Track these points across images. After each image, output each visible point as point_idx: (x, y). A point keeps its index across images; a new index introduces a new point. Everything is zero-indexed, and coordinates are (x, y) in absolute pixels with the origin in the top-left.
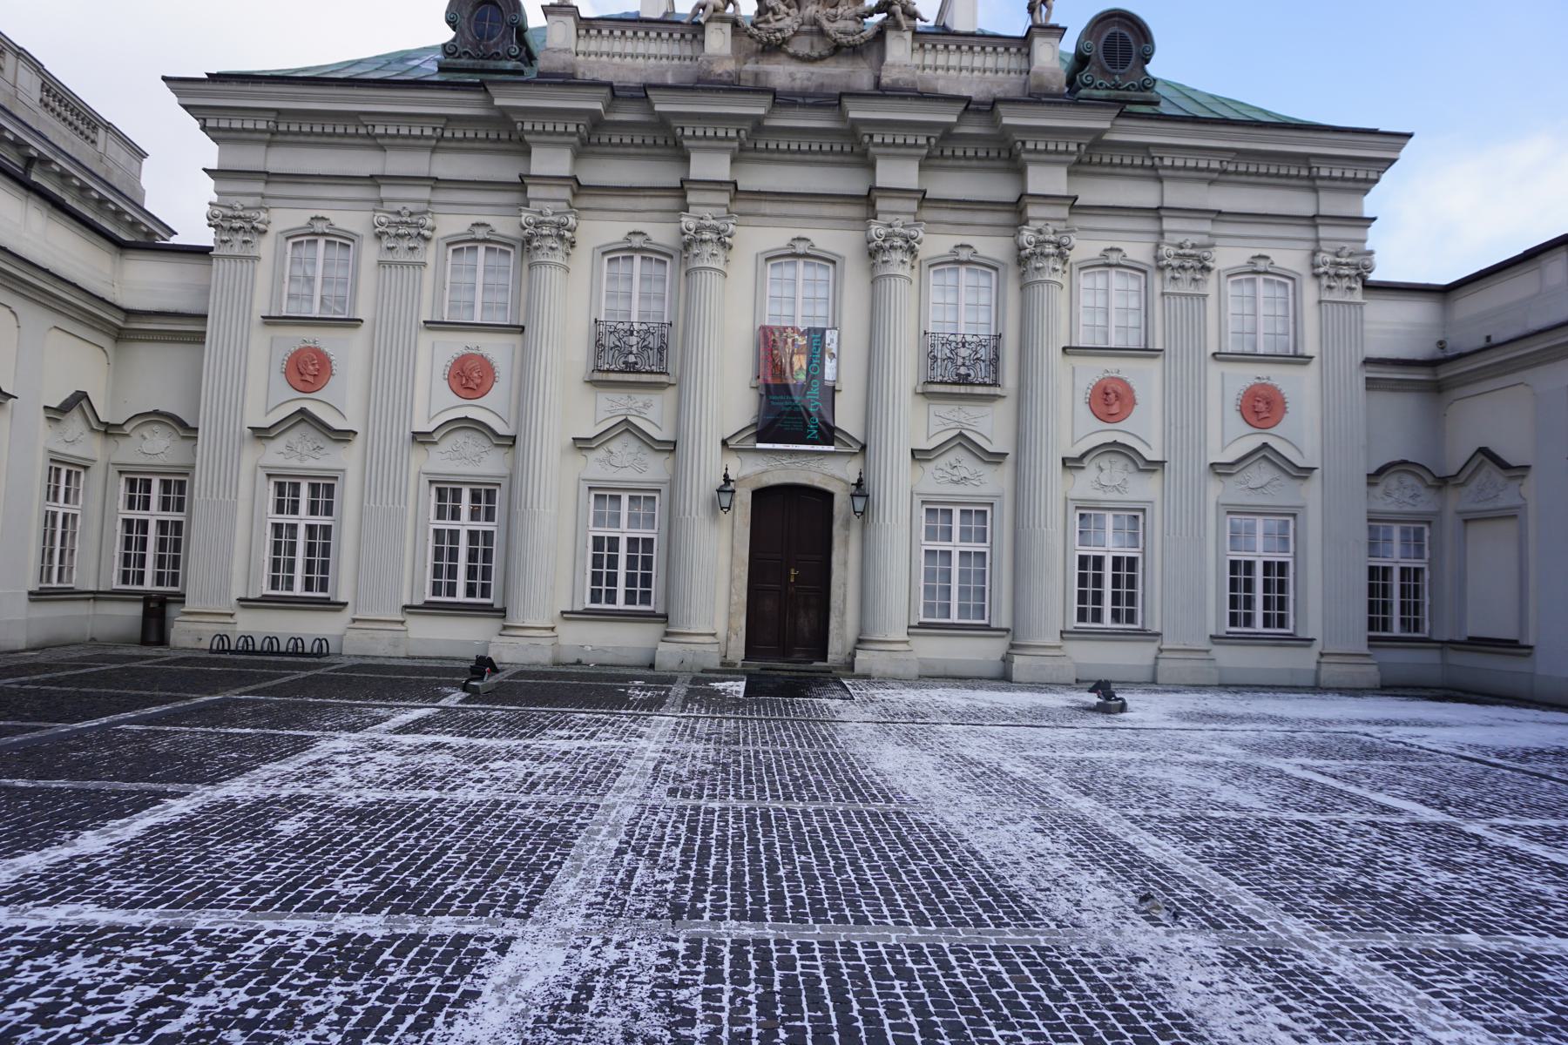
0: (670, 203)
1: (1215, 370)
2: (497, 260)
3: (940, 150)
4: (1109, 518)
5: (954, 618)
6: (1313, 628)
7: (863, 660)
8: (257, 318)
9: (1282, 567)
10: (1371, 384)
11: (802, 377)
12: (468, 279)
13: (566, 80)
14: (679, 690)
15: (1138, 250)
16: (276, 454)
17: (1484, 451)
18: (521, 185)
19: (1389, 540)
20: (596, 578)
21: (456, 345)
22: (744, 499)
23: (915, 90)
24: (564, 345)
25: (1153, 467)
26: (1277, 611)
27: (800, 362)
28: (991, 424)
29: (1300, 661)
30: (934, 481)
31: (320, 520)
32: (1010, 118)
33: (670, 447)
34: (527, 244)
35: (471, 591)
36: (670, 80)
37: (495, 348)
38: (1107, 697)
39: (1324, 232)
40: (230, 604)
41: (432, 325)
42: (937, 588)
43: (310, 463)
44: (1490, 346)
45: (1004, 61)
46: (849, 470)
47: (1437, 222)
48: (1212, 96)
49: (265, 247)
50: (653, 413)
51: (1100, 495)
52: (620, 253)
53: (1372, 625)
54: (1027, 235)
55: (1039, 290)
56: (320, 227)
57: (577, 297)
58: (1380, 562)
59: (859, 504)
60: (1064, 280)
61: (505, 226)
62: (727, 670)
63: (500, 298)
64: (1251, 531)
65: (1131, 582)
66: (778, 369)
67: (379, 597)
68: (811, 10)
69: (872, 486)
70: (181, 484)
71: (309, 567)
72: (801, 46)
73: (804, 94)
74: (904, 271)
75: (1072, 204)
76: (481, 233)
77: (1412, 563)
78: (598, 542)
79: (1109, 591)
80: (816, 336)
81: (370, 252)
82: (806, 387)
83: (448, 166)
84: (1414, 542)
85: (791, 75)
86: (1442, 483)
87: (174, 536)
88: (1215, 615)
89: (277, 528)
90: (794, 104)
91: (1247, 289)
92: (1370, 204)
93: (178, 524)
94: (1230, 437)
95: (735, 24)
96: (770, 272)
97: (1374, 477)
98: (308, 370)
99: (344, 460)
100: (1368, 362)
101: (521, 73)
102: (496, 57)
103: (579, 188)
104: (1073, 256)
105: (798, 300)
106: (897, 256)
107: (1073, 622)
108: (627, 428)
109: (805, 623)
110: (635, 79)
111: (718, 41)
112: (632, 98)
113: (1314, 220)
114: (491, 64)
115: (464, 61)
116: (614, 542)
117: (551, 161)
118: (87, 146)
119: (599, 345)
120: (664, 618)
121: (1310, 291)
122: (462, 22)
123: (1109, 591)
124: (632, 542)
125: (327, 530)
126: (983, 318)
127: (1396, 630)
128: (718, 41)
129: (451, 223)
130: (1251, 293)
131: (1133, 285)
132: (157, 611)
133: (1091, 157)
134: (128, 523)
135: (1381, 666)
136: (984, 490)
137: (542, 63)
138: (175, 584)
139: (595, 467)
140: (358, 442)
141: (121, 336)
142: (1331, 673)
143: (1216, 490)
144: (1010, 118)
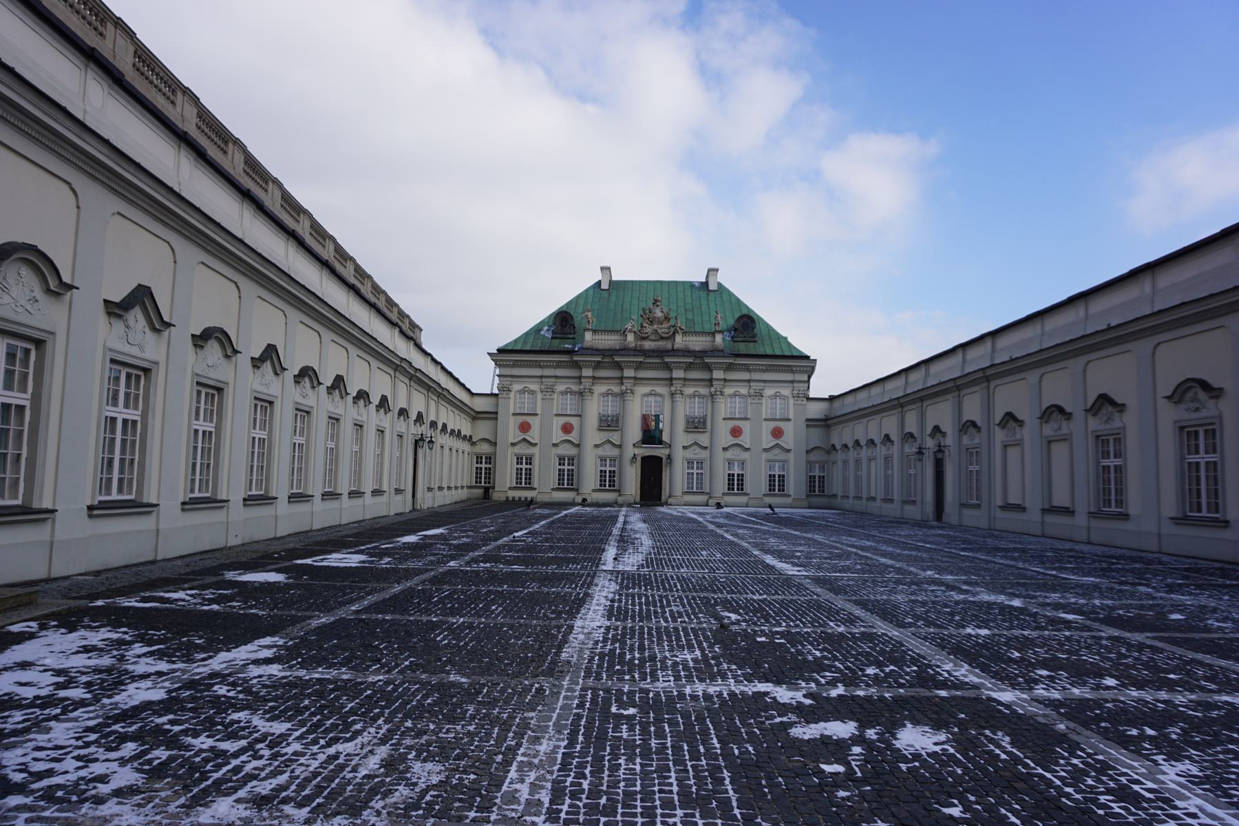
1: (765, 423)
3: (689, 367)
7: (670, 501)
15: (744, 391)
16: (517, 450)
21: (563, 420)
22: (639, 459)
24: (592, 420)
28: (704, 439)
29: (789, 501)
30: (689, 454)
33: (620, 446)
34: (581, 394)
37: (574, 421)
38: (719, 506)
42: (690, 483)
45: (709, 338)
46: (667, 452)
47: (822, 385)
49: (512, 395)
50: (615, 437)
52: (607, 394)
54: (713, 389)
57: (594, 408)
61: (575, 388)
67: (545, 485)
69: (673, 457)
72: (653, 337)
73: (653, 351)
75: (725, 380)
79: (736, 483)
81: (539, 396)
83: (560, 372)
84: (823, 468)
86: (828, 452)
88: (764, 488)
94: (768, 441)
97: (808, 452)
98: (525, 427)
100: (807, 420)
108: (609, 441)
111: (630, 337)
113: (792, 382)
117: (587, 372)
119: (601, 420)
121: (791, 401)
123: (736, 483)
128: (630, 338)
129: (560, 387)
132: (487, 490)
133: (729, 368)
137: (586, 345)
139: (600, 452)
141: (474, 418)
143: (765, 456)
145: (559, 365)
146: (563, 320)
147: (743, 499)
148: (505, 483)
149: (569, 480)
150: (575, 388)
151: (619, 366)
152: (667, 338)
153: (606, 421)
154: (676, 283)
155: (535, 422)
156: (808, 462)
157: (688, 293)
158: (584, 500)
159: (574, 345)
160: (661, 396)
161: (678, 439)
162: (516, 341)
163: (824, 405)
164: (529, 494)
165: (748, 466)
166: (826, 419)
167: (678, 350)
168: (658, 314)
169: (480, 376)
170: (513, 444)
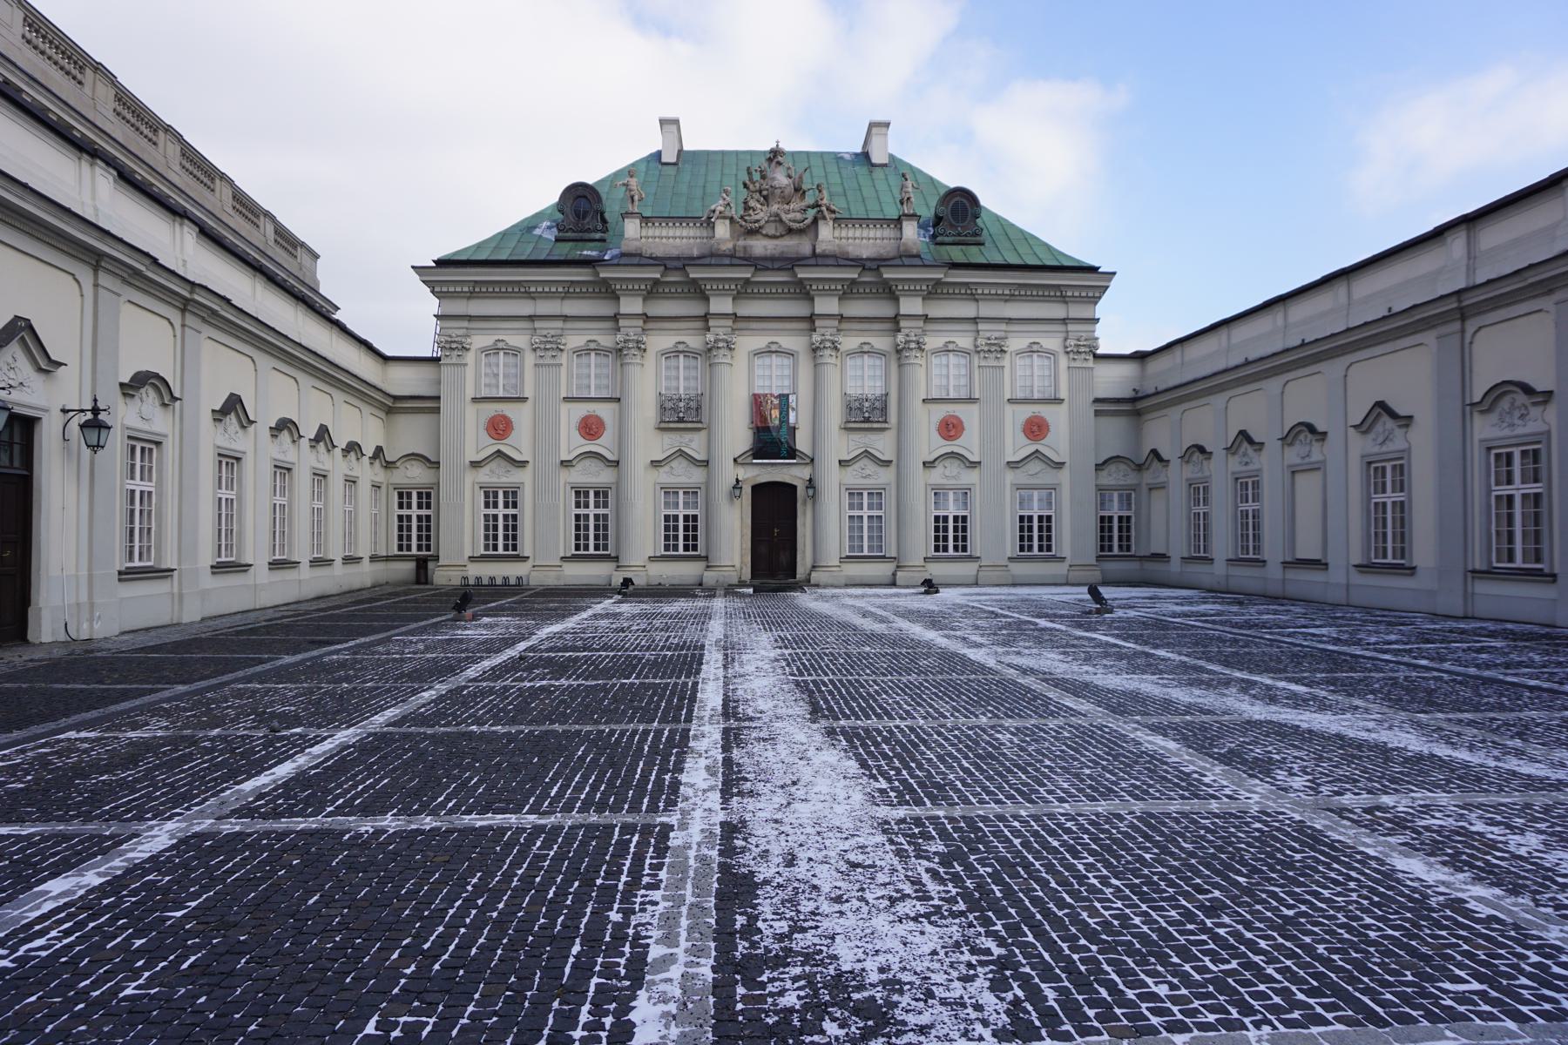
0: (699, 324)
1: (1009, 408)
2: (603, 360)
3: (849, 291)
4: (951, 494)
5: (866, 553)
6: (1066, 552)
8: (468, 398)
9: (1049, 518)
10: (1097, 413)
11: (777, 422)
12: (585, 371)
13: (635, 258)
14: (720, 592)
15: (965, 342)
17: (1155, 453)
18: (615, 318)
19: (1111, 501)
20: (667, 538)
21: (582, 410)
23: (835, 256)
24: (643, 410)
25: (974, 465)
26: (1046, 543)
27: (775, 413)
28: (882, 445)
29: (1059, 569)
30: (852, 477)
31: (511, 511)
32: (888, 274)
33: (706, 464)
34: (619, 352)
35: (597, 548)
36: (696, 253)
37: (605, 411)
38: (930, 586)
39: (1071, 327)
40: (465, 561)
41: (566, 399)
42: (855, 538)
43: (504, 479)
44: (1157, 393)
45: (888, 232)
46: (805, 473)
47: (1128, 323)
48: (1022, 231)
49: (470, 358)
50: (695, 444)
51: (944, 481)
52: (674, 353)
53: (1102, 548)
54: (900, 338)
55: (908, 368)
56: (500, 345)
57: (649, 381)
58: (1106, 513)
59: (811, 492)
60: (923, 362)
61: (606, 341)
62: (742, 584)
63: (605, 382)
64: (1031, 499)
65: (964, 529)
66: (763, 418)
67: (547, 553)
68: (775, 208)
69: (817, 483)
70: (428, 495)
71: (506, 537)
73: (772, 259)
74: (833, 360)
75: (926, 318)
76: (592, 346)
77: (1125, 513)
78: (667, 518)
79: (952, 536)
80: (784, 398)
81: (530, 359)
82: (780, 427)
84: (1126, 501)
85: (765, 248)
86: (1139, 468)
87: (426, 524)
88: (1010, 545)
89: (486, 516)
90: (767, 269)
91: (1028, 361)
92: (1101, 310)
93: (428, 518)
94: (1016, 445)
95: (731, 219)
96: (758, 361)
98: (499, 427)
99: (523, 477)
100: (1097, 401)
101: (603, 240)
102: (588, 231)
103: (646, 318)
104: (926, 347)
105: (773, 378)
106: (827, 352)
107: (932, 553)
108: (681, 454)
109: (784, 558)
110: (675, 253)
111: (722, 230)
112: (676, 269)
113: (1064, 321)
114: (587, 236)
115: (569, 235)
116: (676, 518)
117: (631, 305)
118: (291, 260)
119: (663, 409)
120: (707, 558)
121: (1063, 362)
122: (567, 210)
123: (952, 536)
124: (686, 518)
125: (515, 517)
126: (878, 384)
127: (1116, 551)
128: (722, 230)
129: (575, 340)
130: (1031, 364)
131: (963, 361)
132: (422, 564)
133: (935, 291)
134: (400, 518)
135: (1102, 571)
136: (880, 481)
138: (428, 549)
139: (664, 476)
140: (530, 467)
141: (390, 411)
142: (1076, 575)
143: (1010, 477)
144: (888, 274)
145: (569, 292)
146: (581, 205)
147: (968, 569)
148: (461, 550)
149: (596, 535)
150: (606, 341)
151: (699, 292)
152: (801, 232)
153: (675, 409)
154: (808, 154)
155: (521, 416)
156: (1100, 489)
157: (832, 168)
158: (627, 582)
159: (605, 251)
160: (791, 354)
161: (830, 446)
162: (479, 246)
163: (1127, 370)
164: (512, 571)
165: (977, 497)
166: (1133, 400)
167: (824, 256)
168: (781, 179)
169: (404, 320)
170: (475, 465)
